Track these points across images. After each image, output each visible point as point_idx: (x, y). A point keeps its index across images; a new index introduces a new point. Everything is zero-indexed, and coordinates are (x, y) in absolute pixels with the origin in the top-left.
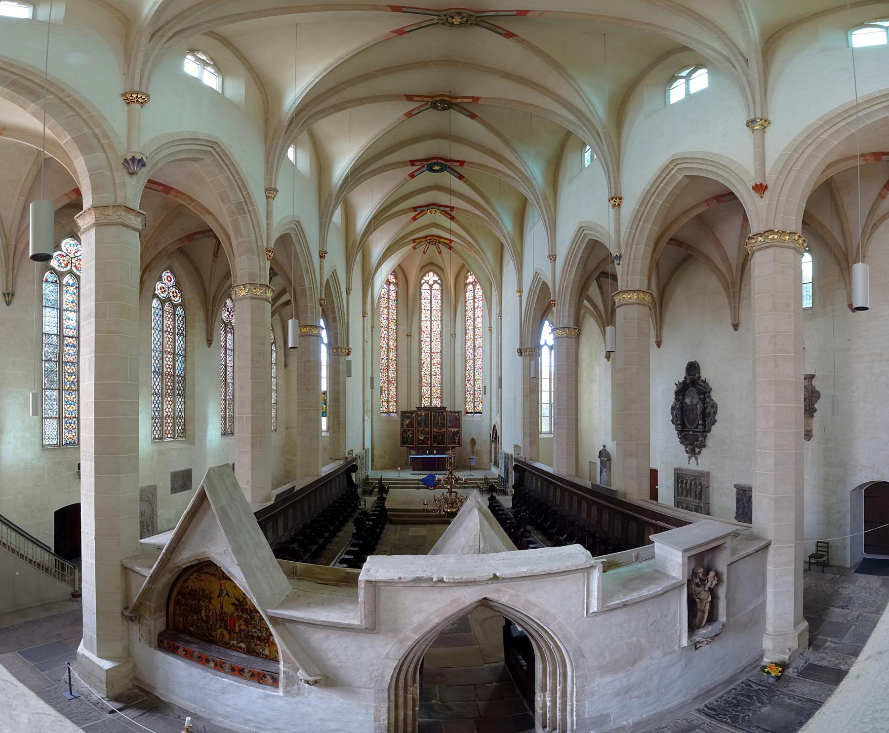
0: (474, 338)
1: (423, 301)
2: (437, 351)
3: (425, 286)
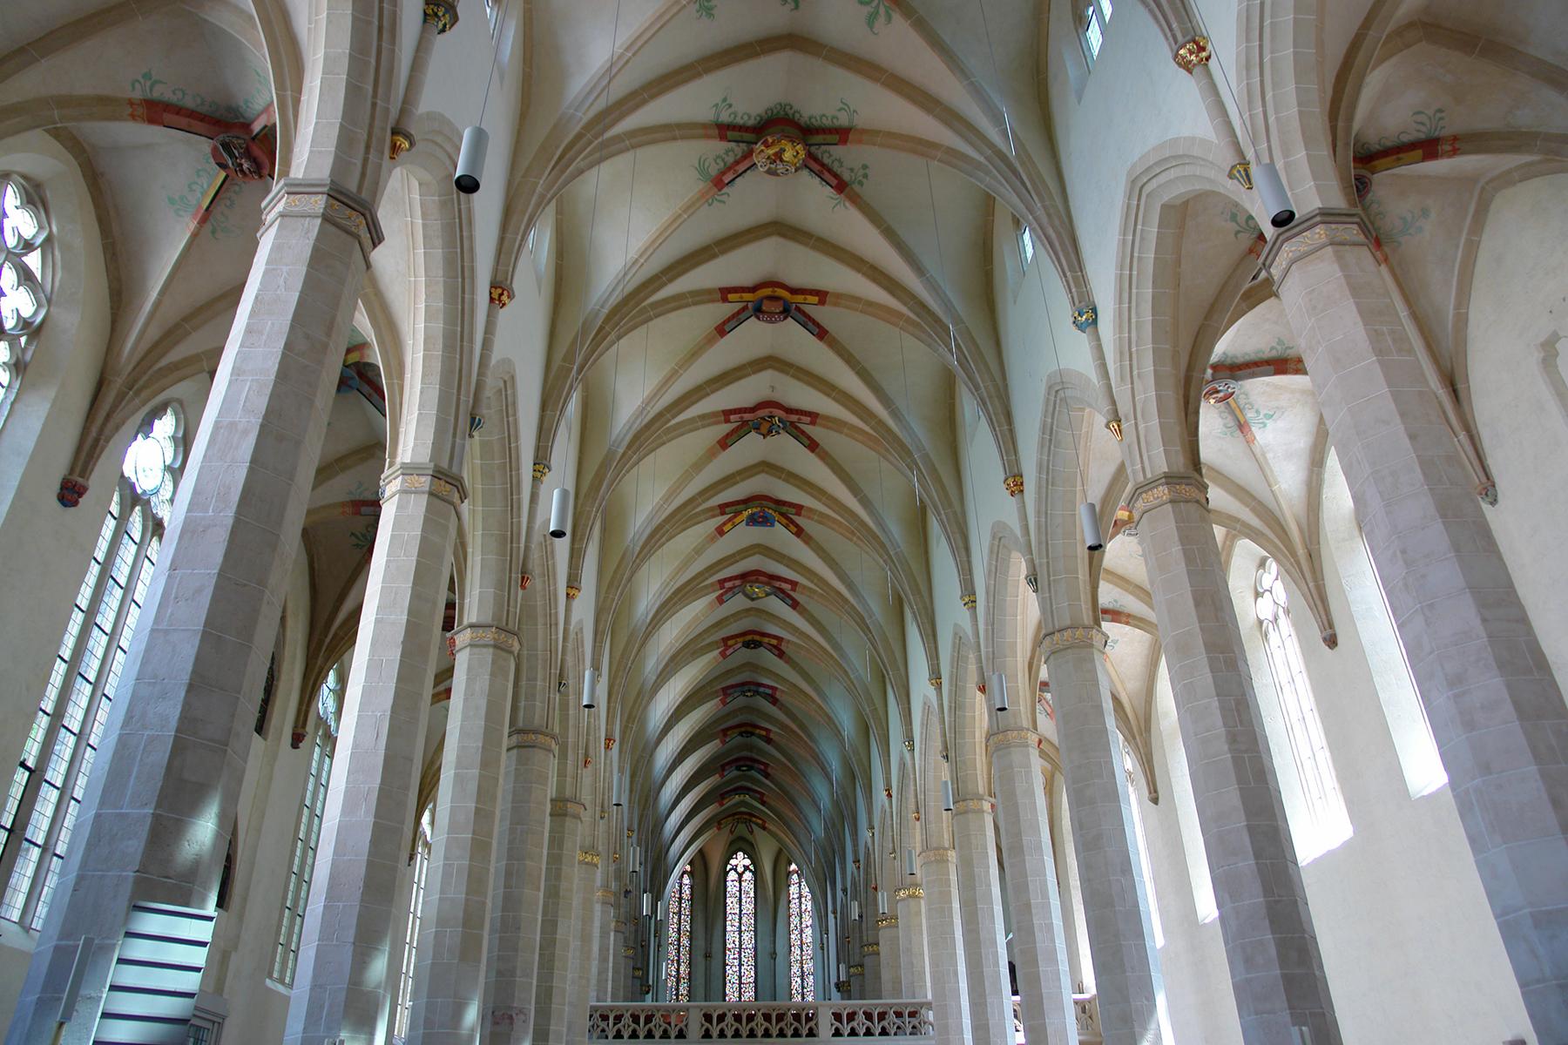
1: (729, 901)
2: (748, 980)
3: (732, 876)
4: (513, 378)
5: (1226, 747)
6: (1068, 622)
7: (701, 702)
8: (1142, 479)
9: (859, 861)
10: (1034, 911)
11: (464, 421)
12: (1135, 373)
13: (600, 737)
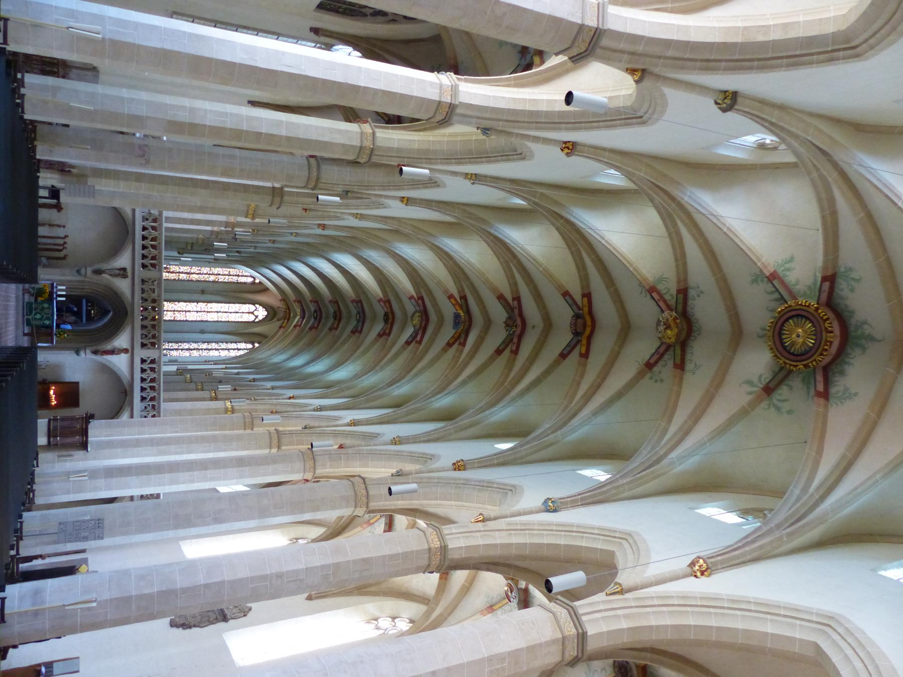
0: (199, 349)
1: (237, 305)
3: (251, 308)
4: (524, 159)
5: (274, 571)
6: (371, 493)
7: (352, 287)
8: (445, 533)
9: (254, 381)
10: (202, 472)
11: (488, 124)
12: (512, 532)
13: (325, 220)
